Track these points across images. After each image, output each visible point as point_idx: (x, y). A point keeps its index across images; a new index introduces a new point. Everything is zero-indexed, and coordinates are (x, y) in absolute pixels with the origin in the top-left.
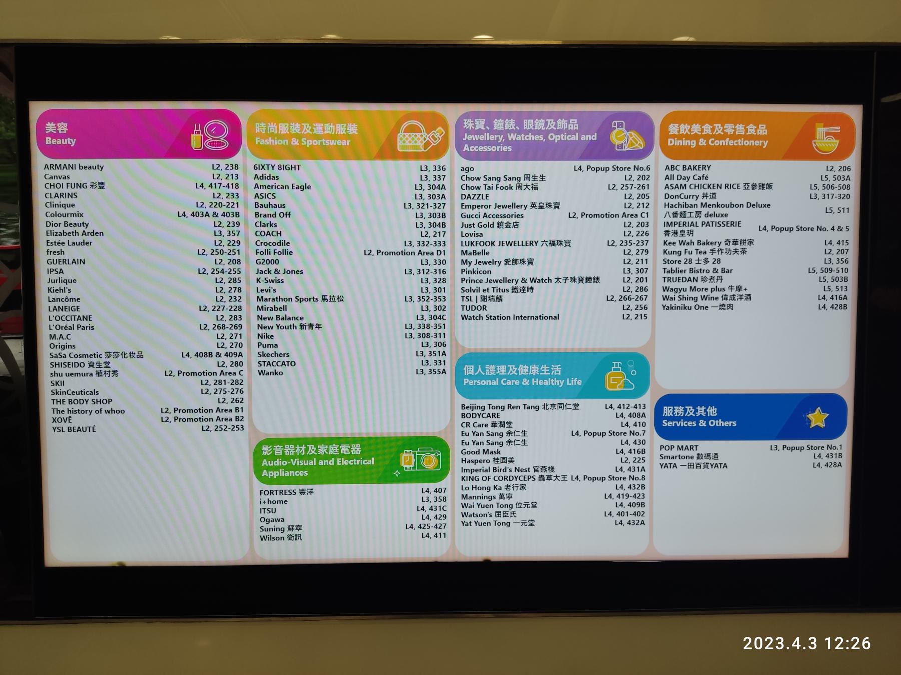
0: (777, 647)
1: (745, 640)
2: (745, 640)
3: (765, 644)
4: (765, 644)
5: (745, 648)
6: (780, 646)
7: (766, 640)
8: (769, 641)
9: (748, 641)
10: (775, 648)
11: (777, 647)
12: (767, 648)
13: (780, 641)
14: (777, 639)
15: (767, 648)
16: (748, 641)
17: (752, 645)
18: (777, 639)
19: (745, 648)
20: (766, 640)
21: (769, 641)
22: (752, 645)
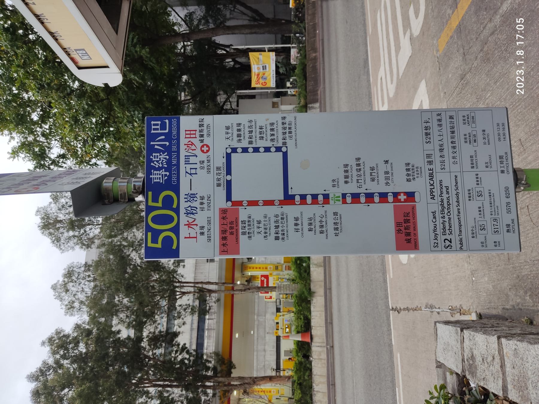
0: (522, 74)
1: (518, 93)
2: (518, 93)
3: (521, 81)
4: (521, 81)
5: (523, 93)
6: (522, 72)
7: (518, 81)
8: (519, 79)
9: (518, 92)
10: (523, 76)
11: (522, 74)
12: (523, 80)
13: (518, 72)
14: (518, 74)
15: (523, 80)
16: (518, 92)
17: (521, 89)
18: (518, 74)
19: (523, 93)
20: (518, 81)
21: (519, 79)
22: (521, 89)
